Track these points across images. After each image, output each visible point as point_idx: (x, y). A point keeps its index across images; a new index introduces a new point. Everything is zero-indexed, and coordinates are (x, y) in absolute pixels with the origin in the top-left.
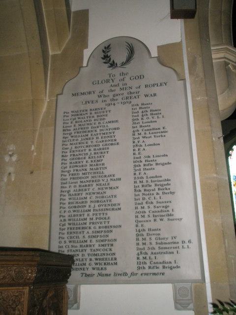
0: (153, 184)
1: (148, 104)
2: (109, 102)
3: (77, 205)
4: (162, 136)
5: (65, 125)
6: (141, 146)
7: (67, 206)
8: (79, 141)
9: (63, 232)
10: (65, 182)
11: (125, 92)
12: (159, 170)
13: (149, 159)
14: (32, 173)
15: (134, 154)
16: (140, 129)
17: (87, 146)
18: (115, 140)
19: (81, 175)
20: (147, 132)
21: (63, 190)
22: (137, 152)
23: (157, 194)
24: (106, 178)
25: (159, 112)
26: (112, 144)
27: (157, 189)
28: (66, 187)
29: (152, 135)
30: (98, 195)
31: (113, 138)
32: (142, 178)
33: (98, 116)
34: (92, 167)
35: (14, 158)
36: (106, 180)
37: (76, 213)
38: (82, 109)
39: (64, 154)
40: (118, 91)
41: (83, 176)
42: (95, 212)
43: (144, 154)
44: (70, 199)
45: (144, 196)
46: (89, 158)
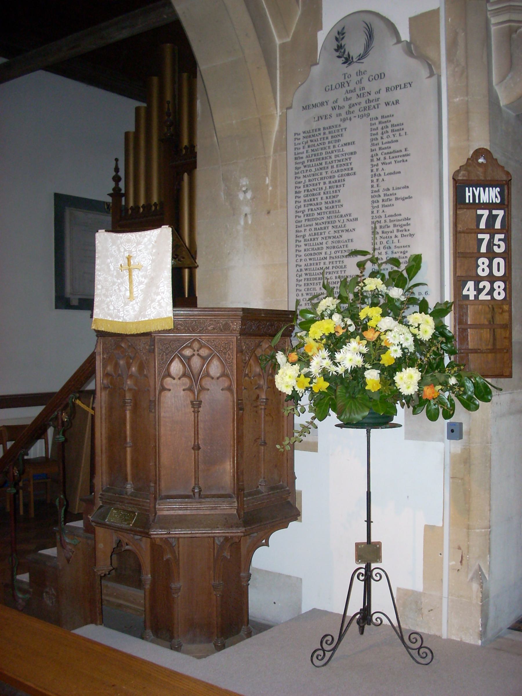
0: (391, 225)
1: (388, 116)
2: (344, 116)
3: (313, 252)
4: (403, 161)
5: (297, 151)
6: (380, 175)
7: (302, 253)
8: (313, 173)
9: (300, 283)
10: (299, 224)
11: (363, 100)
12: (399, 207)
13: (388, 193)
14: (269, 213)
15: (372, 186)
16: (379, 152)
17: (321, 179)
18: (352, 169)
19: (316, 216)
20: (387, 156)
21: (299, 234)
22: (375, 184)
23: (396, 237)
24: (342, 219)
25: (401, 127)
26: (348, 175)
27: (395, 231)
28: (301, 231)
29: (393, 160)
30: (334, 240)
31: (350, 167)
32: (381, 217)
33: (332, 137)
34: (327, 206)
35: (249, 195)
36: (342, 221)
37: (312, 262)
38: (314, 128)
39: (297, 190)
40: (355, 100)
41: (319, 216)
42: (331, 260)
43: (383, 185)
44: (306, 245)
45: (382, 240)
46: (324, 193)
